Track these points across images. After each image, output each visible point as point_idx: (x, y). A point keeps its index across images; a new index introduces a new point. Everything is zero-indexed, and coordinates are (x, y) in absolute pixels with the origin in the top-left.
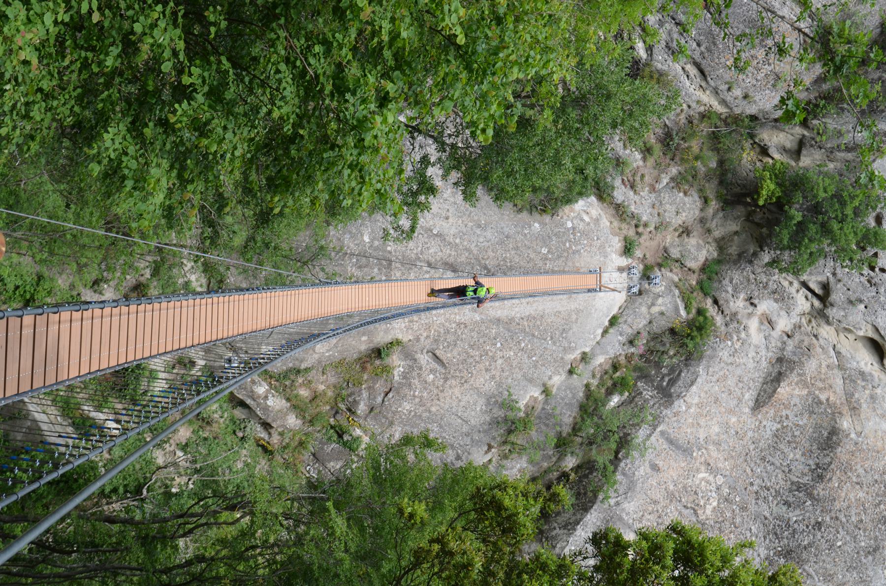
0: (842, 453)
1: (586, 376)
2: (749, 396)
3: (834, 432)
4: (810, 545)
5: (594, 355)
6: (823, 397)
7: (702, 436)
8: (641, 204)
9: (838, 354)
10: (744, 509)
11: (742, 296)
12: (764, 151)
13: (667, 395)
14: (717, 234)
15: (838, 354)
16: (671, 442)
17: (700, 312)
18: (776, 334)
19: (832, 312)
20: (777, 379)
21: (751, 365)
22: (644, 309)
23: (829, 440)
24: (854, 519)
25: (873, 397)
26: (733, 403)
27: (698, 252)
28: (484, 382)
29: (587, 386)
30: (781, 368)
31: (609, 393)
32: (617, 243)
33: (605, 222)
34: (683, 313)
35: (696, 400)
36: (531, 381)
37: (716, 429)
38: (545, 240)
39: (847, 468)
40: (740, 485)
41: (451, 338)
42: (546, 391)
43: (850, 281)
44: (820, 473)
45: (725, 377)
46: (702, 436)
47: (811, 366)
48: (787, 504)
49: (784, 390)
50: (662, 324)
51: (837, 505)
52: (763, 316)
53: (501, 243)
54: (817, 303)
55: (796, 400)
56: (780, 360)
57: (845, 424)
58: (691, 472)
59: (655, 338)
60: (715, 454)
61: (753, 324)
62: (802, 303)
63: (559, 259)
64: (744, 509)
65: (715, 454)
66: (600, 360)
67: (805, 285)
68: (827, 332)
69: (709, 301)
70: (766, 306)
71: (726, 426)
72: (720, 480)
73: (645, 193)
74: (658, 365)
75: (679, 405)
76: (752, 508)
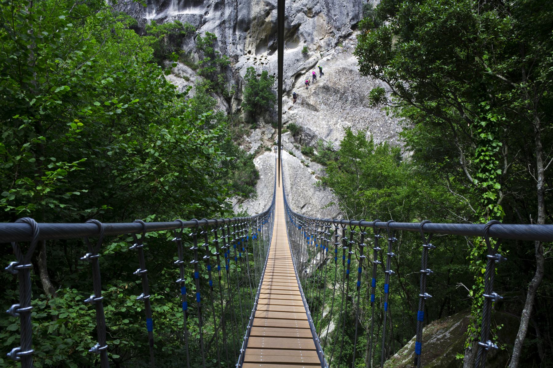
0: (330, 85)
1: (308, 161)
3: (324, 87)
4: (359, 94)
5: (302, 159)
6: (313, 91)
7: (326, 126)
8: (255, 147)
9: (300, 87)
10: (348, 114)
13: (313, 137)
15: (300, 87)
16: (328, 135)
17: (288, 128)
20: (308, 104)
21: (304, 112)
22: (287, 144)
24: (350, 81)
26: (316, 117)
27: (270, 130)
28: (310, 192)
29: (311, 161)
31: (313, 155)
32: (267, 153)
33: (261, 156)
34: (289, 132)
35: (315, 128)
36: (310, 178)
37: (324, 122)
38: (266, 174)
39: (335, 83)
40: (341, 115)
41: (297, 202)
42: (313, 173)
44: (336, 91)
45: (308, 120)
46: (326, 126)
48: (346, 101)
49: (311, 102)
51: (346, 86)
53: (267, 187)
55: (314, 99)
56: (302, 104)
58: (337, 129)
60: (331, 123)
61: (291, 112)
64: (348, 114)
65: (331, 123)
66: (303, 157)
69: (285, 125)
71: (323, 119)
72: (339, 121)
73: (252, 145)
74: (305, 140)
76: (348, 111)
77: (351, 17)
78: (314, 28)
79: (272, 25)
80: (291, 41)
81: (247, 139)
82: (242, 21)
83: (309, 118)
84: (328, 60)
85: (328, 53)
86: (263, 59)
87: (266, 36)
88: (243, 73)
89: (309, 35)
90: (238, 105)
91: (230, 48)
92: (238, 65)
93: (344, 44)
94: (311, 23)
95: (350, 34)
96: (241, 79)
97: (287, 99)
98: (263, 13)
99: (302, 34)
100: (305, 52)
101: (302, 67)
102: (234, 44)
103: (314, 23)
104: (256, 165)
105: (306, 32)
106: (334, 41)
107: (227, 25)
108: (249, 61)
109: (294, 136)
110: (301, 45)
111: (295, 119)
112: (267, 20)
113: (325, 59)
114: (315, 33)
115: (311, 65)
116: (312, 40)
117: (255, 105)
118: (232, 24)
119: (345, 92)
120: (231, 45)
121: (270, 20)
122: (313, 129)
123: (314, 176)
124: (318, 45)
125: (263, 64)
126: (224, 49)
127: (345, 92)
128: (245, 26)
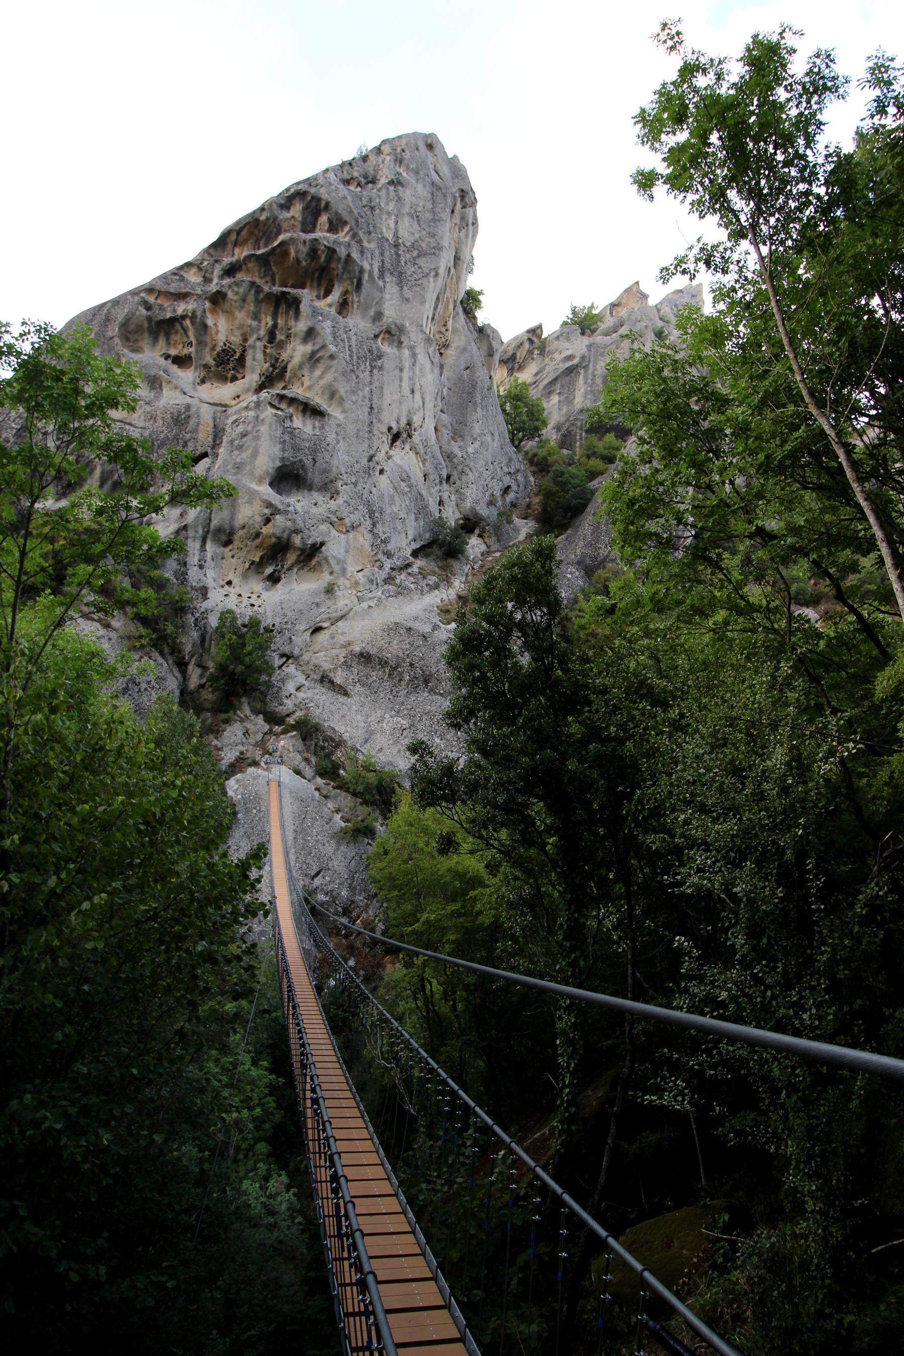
0: (373, 651)
1: (329, 789)
2: (342, 699)
6: (343, 660)
10: (403, 703)
11: (285, 701)
12: (202, 686)
13: (339, 743)
14: (248, 713)
16: (366, 741)
18: (307, 683)
19: (296, 652)
20: (331, 682)
21: (324, 697)
22: (291, 755)
23: (365, 658)
25: (342, 634)
27: (259, 724)
29: (334, 788)
30: (325, 680)
31: (338, 775)
33: (239, 776)
37: (359, 717)
38: (247, 811)
39: (381, 649)
40: (390, 705)
41: (304, 867)
42: (338, 811)
43: (279, 642)
44: (383, 663)
45: (331, 711)
47: (326, 666)
48: (400, 680)
49: (338, 680)
50: (300, 744)
51: (401, 654)
52: (296, 691)
53: (249, 837)
54: (290, 661)
55: (344, 674)
57: (357, 649)
58: (383, 731)
59: (308, 749)
61: (301, 695)
62: (291, 669)
63: (255, 800)
64: (403, 703)
67: (280, 667)
68: (306, 657)
70: (290, 687)
72: (387, 716)
74: (323, 748)
75: (346, 736)
76: (401, 699)
77: (410, 537)
78: (347, 551)
79: (274, 540)
80: (306, 569)
81: (215, 742)
82: (219, 530)
83: (333, 708)
84: (370, 607)
85: (370, 595)
86: (254, 597)
87: (262, 558)
88: (213, 621)
89: (339, 561)
90: (201, 676)
91: (193, 573)
92: (205, 605)
93: (398, 581)
94: (343, 543)
95: (409, 565)
96: (209, 630)
97: (294, 671)
98: (258, 519)
99: (326, 559)
100: (330, 590)
101: (323, 616)
102: (201, 567)
103: (347, 542)
104: (230, 793)
105: (334, 557)
106: (383, 575)
107: (191, 533)
108: (227, 599)
109: (304, 739)
110: (326, 578)
111: (308, 709)
112: (265, 530)
113: (365, 605)
114: (350, 560)
115: (339, 614)
116: (344, 571)
117: (232, 678)
118: (201, 531)
119: (398, 666)
120: (195, 568)
121: (271, 531)
122: (340, 728)
123: (337, 817)
124: (353, 580)
125: (253, 605)
126: (182, 576)
127: (398, 666)
128: (224, 538)
